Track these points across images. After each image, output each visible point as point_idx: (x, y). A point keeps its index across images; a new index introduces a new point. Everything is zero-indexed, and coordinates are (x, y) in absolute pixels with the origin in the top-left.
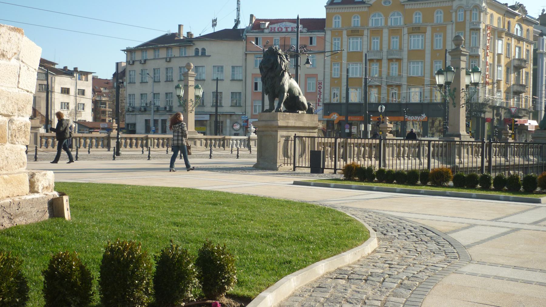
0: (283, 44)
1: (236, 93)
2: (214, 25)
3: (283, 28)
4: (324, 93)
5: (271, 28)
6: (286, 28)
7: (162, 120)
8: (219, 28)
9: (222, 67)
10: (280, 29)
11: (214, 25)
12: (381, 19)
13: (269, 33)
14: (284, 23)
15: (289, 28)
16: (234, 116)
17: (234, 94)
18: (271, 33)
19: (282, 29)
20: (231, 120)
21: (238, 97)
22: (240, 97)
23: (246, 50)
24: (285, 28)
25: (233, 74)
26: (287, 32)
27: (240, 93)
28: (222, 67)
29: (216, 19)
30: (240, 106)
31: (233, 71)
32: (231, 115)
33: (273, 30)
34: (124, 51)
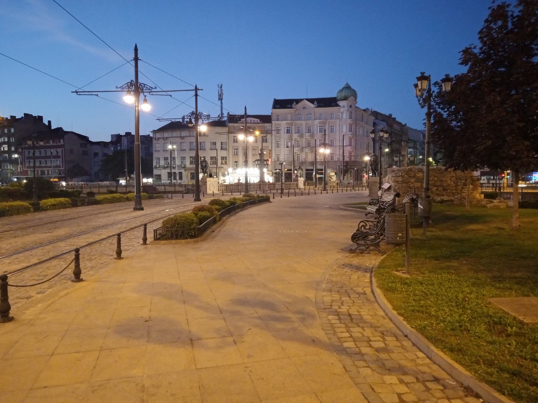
1: (224, 157)
6: (251, 121)
7: (179, 172)
12: (302, 117)
22: (226, 159)
26: (251, 123)
27: (226, 157)
28: (215, 143)
34: (151, 132)
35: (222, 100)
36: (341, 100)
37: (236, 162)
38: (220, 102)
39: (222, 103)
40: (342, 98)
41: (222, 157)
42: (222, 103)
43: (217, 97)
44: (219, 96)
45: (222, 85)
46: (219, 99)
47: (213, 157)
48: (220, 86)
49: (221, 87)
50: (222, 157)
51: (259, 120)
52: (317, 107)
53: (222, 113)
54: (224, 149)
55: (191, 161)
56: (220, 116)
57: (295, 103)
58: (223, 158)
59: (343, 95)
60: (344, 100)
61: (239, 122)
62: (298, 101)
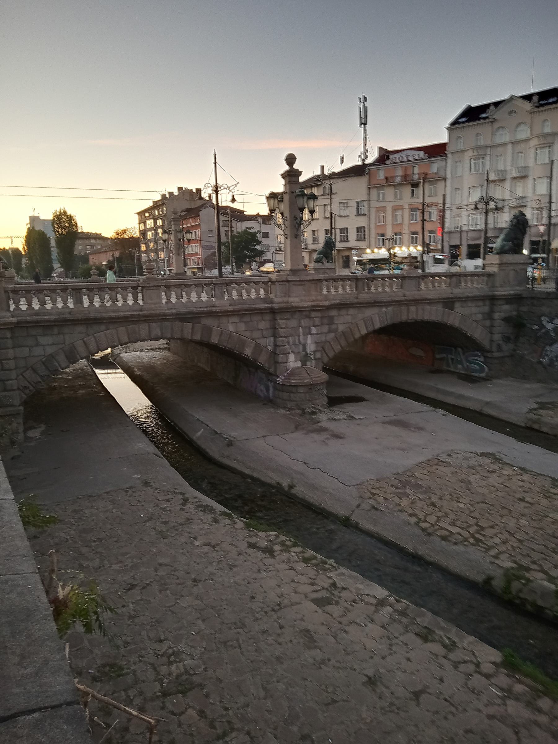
0: (213, 182)
2: (342, 161)
3: (404, 156)
5: (392, 158)
6: (407, 157)
8: (347, 165)
11: (342, 161)
14: (405, 152)
23: (369, 185)
27: (364, 227)
33: (394, 160)
35: (365, 124)
37: (383, 235)
38: (362, 129)
41: (358, 228)
46: (361, 124)
47: (344, 228)
50: (358, 228)
51: (422, 153)
52: (537, 107)
54: (360, 215)
55: (314, 238)
57: (492, 108)
61: (388, 162)
62: (497, 104)
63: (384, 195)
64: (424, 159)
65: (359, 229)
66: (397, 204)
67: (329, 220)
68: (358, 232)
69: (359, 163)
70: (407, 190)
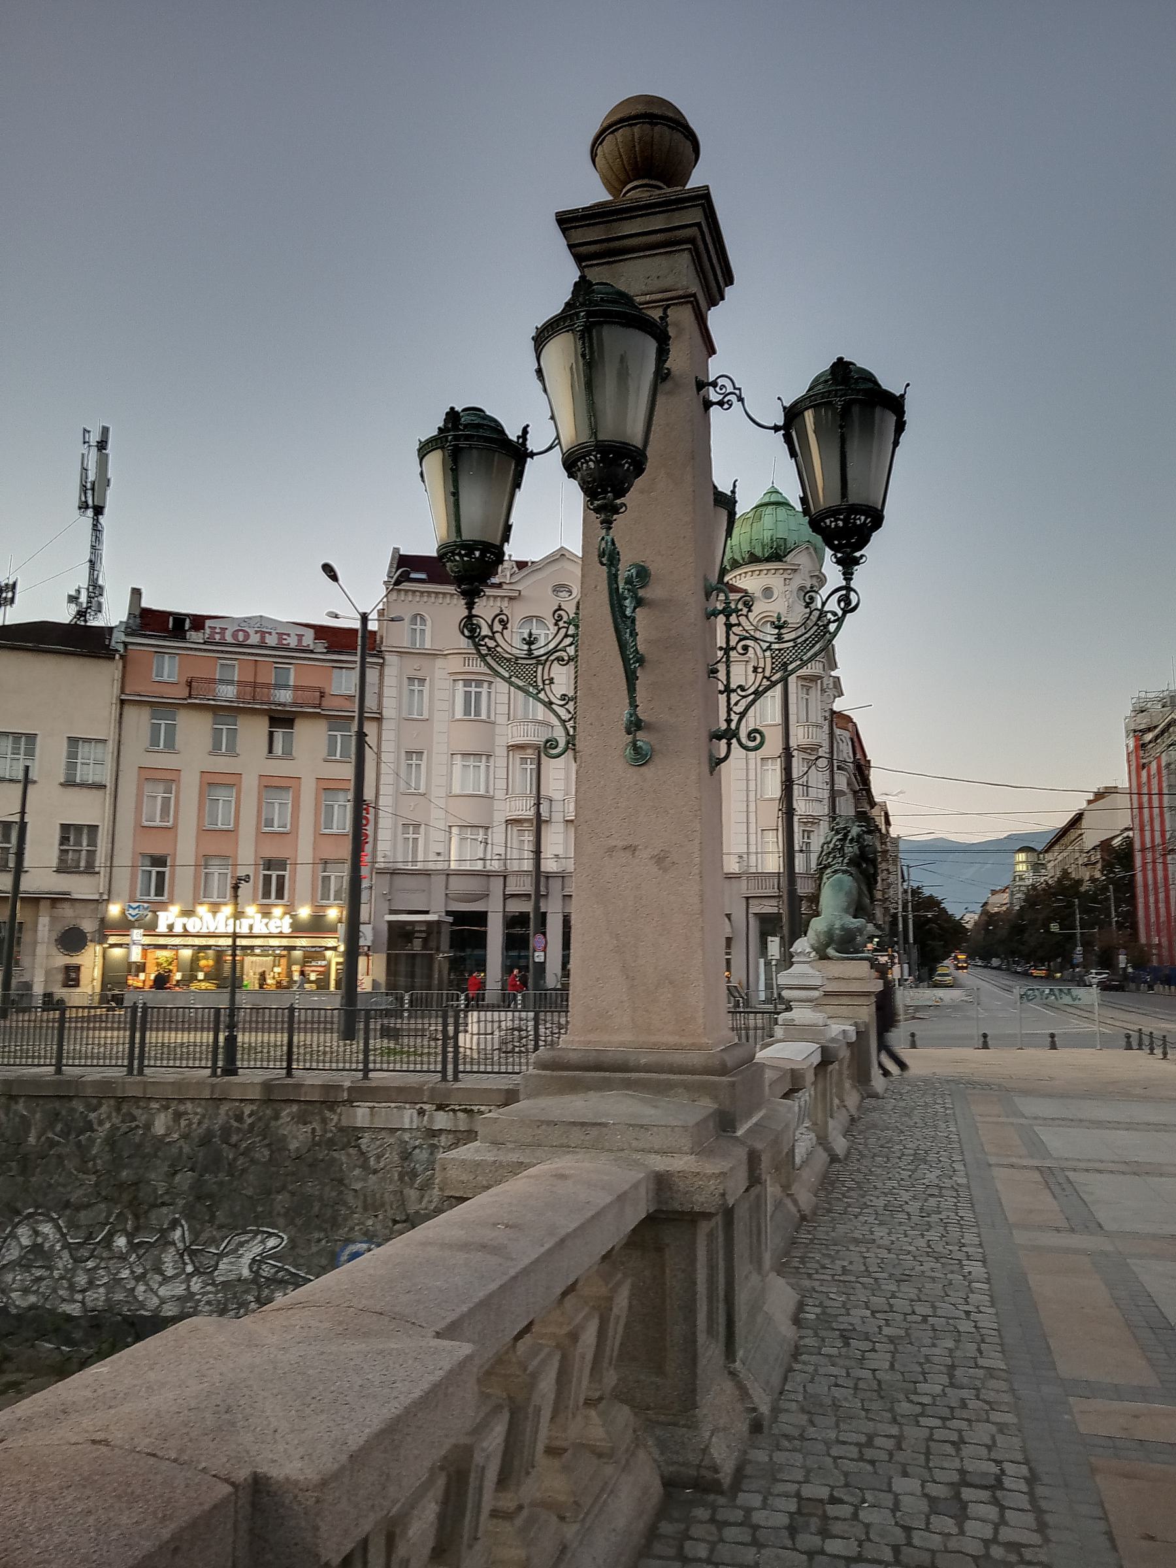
1: (79, 828)
3: (251, 631)
4: (375, 839)
9: (31, 738)
10: (241, 636)
13: (204, 643)
15: (270, 633)
16: (66, 905)
17: (72, 827)
18: (211, 643)
19: (247, 636)
20: (54, 920)
21: (85, 843)
22: (93, 842)
23: (123, 692)
24: (257, 632)
25: (71, 766)
27: (93, 829)
29: (14, 585)
30: (90, 870)
31: (72, 755)
32: (54, 901)
33: (217, 637)
35: (98, 510)
36: (754, 559)
37: (159, 861)
39: (96, 528)
40: (758, 552)
41: (65, 828)
42: (96, 528)
43: (73, 496)
44: (84, 489)
45: (105, 431)
46: (84, 506)
48: (94, 438)
49: (102, 445)
50: (65, 828)
53: (96, 589)
56: (83, 598)
58: (68, 832)
59: (767, 535)
60: (768, 560)
63: (171, 731)
64: (312, 652)
65: (68, 832)
66: (222, 764)
67: (20, 787)
68: (64, 840)
69: (64, 615)
70: (253, 731)
